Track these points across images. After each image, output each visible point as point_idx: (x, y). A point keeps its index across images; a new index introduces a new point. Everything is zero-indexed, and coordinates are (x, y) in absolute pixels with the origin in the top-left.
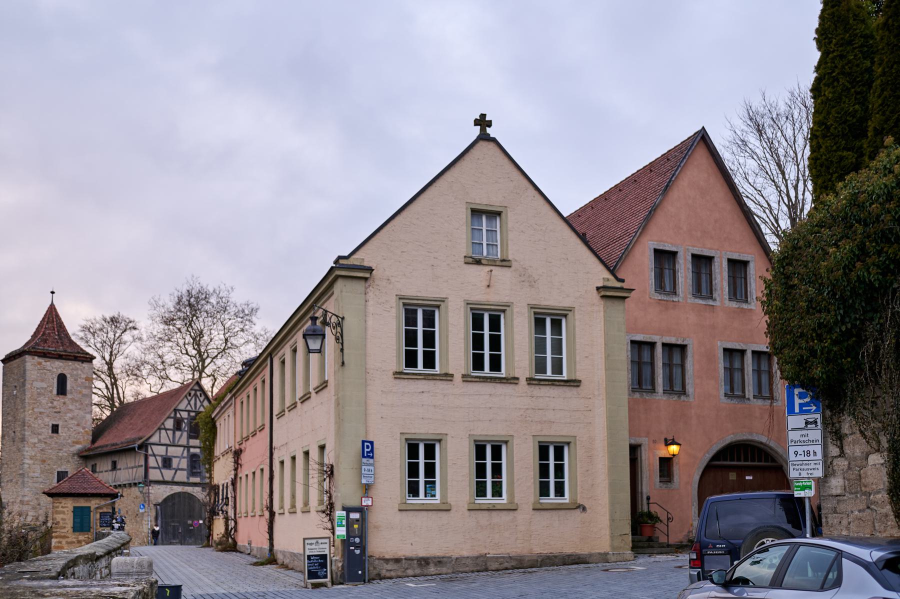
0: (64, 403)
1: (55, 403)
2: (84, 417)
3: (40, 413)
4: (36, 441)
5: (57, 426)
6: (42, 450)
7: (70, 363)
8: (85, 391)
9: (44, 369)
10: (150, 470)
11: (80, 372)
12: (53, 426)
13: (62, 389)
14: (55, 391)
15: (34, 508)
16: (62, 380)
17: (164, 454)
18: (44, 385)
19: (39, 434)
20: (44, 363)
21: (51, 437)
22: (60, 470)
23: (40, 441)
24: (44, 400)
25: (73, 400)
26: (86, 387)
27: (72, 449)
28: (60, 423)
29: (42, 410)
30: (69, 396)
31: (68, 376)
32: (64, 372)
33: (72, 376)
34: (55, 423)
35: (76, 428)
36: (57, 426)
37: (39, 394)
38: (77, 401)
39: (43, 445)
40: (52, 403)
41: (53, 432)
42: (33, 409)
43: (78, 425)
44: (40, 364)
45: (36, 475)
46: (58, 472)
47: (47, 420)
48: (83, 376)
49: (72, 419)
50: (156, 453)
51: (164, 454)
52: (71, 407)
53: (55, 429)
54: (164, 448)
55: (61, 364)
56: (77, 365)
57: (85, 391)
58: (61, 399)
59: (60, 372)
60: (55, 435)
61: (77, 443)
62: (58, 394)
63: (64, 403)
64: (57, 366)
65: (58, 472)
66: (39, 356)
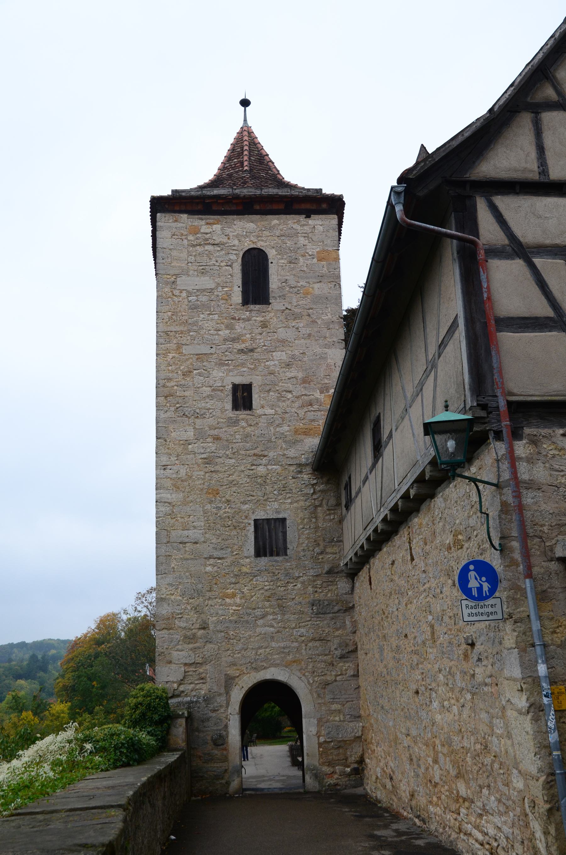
0: (264, 325)
1: (239, 327)
2: (323, 357)
3: (200, 357)
4: (190, 434)
5: (247, 388)
6: (208, 461)
7: (274, 220)
8: (318, 289)
9: (206, 242)
10: (508, 340)
11: (302, 241)
12: (236, 388)
14: (237, 297)
15: (190, 639)
18: (206, 282)
19: (198, 416)
20: (204, 229)
21: (234, 422)
22: (261, 515)
23: (200, 435)
24: (208, 323)
25: (291, 315)
26: (321, 278)
27: (292, 453)
28: (257, 381)
29: (205, 349)
30: (276, 304)
31: (271, 254)
32: (260, 245)
33: (280, 251)
34: (238, 380)
35: (299, 390)
36: (247, 388)
37: (194, 308)
38: (296, 316)
39: (212, 447)
40: (230, 327)
41: (236, 407)
42: (179, 346)
44: (195, 231)
45: (193, 534)
46: (255, 521)
47: (217, 374)
48: (313, 249)
49: (288, 365)
50: (528, 231)
52: (282, 333)
53: (242, 397)
55: (251, 226)
56: (293, 223)
57: (318, 289)
59: (248, 245)
60: (242, 414)
61: (307, 433)
62: (246, 302)
63: (264, 325)
64: (244, 232)
65: (255, 521)
66: (191, 212)
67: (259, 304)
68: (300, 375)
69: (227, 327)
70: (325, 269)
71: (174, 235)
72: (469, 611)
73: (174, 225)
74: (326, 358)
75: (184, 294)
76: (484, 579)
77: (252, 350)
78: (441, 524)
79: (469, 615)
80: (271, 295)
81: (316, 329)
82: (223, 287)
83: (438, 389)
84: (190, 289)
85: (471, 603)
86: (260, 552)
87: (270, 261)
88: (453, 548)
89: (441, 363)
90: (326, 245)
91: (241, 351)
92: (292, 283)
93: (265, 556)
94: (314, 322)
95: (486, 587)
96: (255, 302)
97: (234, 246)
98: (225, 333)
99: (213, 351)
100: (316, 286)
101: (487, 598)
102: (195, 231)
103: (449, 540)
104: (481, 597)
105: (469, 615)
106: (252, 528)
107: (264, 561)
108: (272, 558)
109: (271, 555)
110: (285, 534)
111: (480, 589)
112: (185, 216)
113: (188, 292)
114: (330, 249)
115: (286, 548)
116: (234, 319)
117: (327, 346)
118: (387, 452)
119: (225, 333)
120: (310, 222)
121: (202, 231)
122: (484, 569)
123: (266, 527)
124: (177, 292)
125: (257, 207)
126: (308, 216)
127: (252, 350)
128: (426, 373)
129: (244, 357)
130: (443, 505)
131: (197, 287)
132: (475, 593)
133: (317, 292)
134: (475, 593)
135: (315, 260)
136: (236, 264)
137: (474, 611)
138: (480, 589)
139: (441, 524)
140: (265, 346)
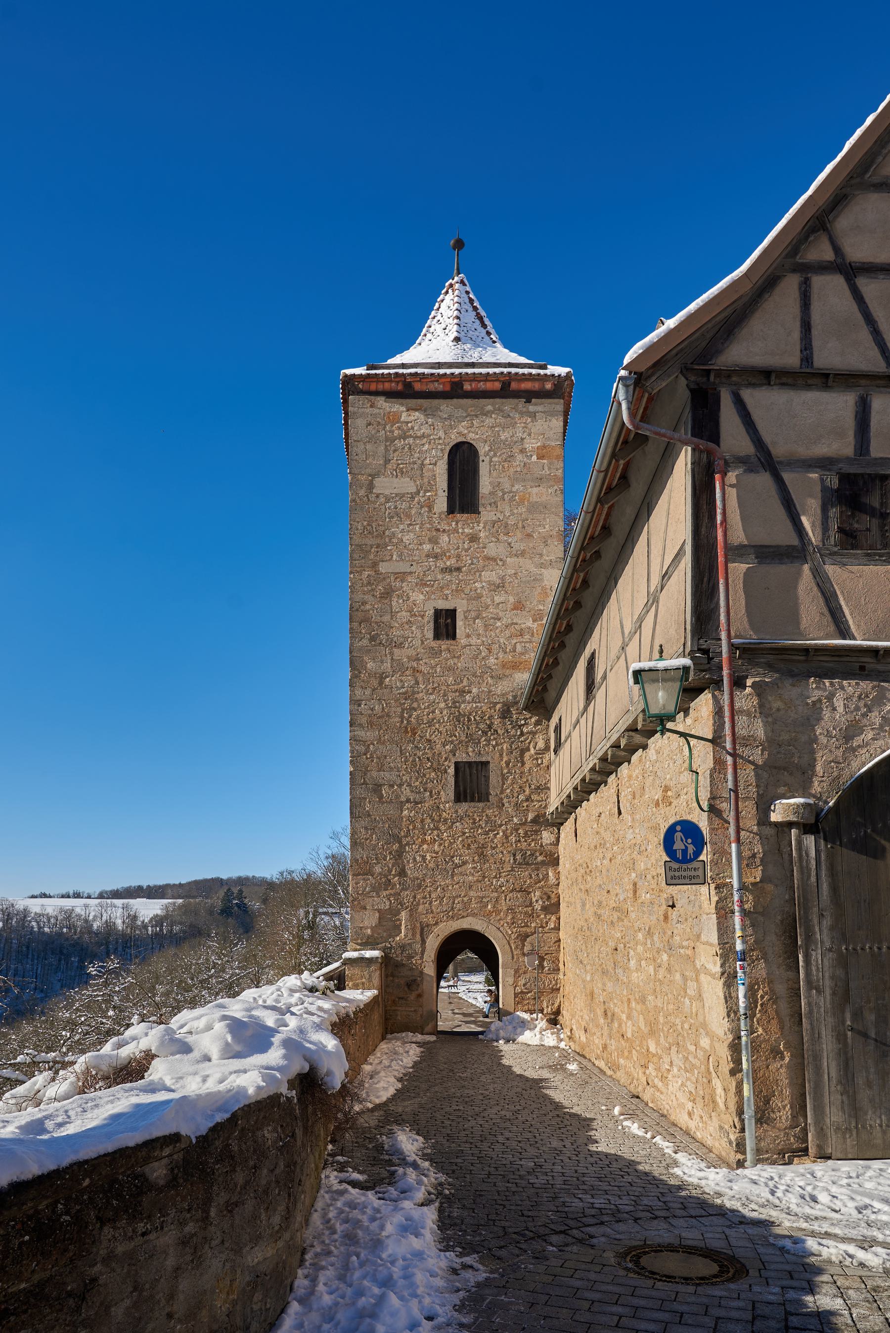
0: (474, 538)
2: (538, 579)
13: (463, 493)
14: (441, 504)
16: (463, 463)
17: (842, 446)
29: (403, 567)
30: (487, 514)
31: (483, 449)
32: (471, 437)
40: (434, 541)
43: (519, 606)
51: (842, 446)
52: (492, 550)
54: (840, 405)
58: (464, 524)
59: (454, 439)
62: (451, 510)
67: (468, 513)
68: (511, 599)
69: (430, 540)
70: (546, 468)
71: (370, 424)
72: (672, 873)
73: (369, 410)
74: (542, 580)
75: (382, 500)
76: (690, 841)
77: (458, 569)
78: (651, 778)
79: (672, 878)
80: (482, 501)
81: (531, 545)
82: (426, 491)
83: (657, 627)
84: (387, 492)
85: (675, 865)
86: (460, 797)
87: (481, 459)
88: (661, 805)
89: (663, 597)
90: (549, 439)
91: (445, 570)
92: (507, 486)
93: (466, 801)
94: (529, 536)
95: (691, 849)
96: (463, 510)
97: (440, 438)
98: (427, 547)
99: (413, 569)
100: (535, 490)
101: (691, 860)
102: (395, 419)
103: (658, 796)
104: (685, 860)
105: (672, 878)
106: (451, 771)
107: (464, 807)
108: (473, 804)
109: (472, 800)
110: (487, 778)
111: (685, 851)
112: (383, 398)
113: (386, 496)
114: (553, 444)
115: (488, 794)
116: (438, 530)
117: (542, 566)
118: (600, 695)
119: (427, 547)
120: (531, 408)
121: (403, 419)
122: (689, 829)
123: (467, 770)
124: (372, 497)
125: (467, 387)
126: (528, 401)
127: (458, 569)
128: (647, 607)
129: (448, 577)
130: (655, 757)
131: (395, 491)
132: (679, 855)
133: (534, 499)
134: (679, 855)
135: (534, 458)
136: (442, 462)
137: (677, 874)
138: (685, 851)
139: (651, 778)
140: (472, 564)
